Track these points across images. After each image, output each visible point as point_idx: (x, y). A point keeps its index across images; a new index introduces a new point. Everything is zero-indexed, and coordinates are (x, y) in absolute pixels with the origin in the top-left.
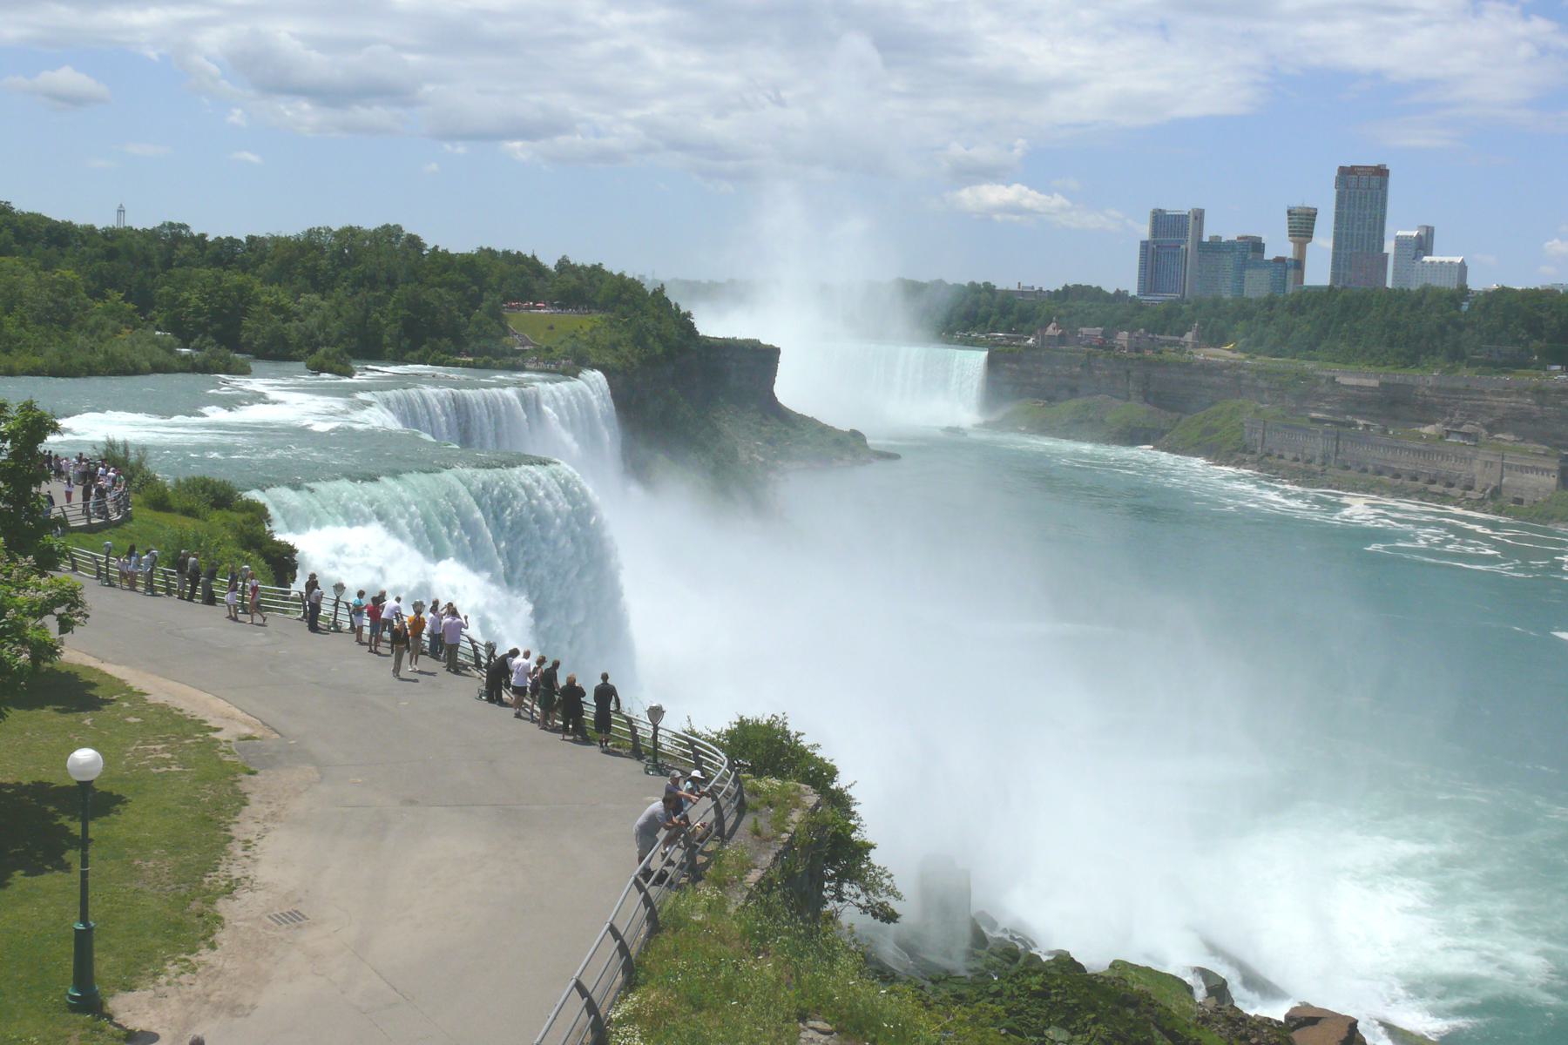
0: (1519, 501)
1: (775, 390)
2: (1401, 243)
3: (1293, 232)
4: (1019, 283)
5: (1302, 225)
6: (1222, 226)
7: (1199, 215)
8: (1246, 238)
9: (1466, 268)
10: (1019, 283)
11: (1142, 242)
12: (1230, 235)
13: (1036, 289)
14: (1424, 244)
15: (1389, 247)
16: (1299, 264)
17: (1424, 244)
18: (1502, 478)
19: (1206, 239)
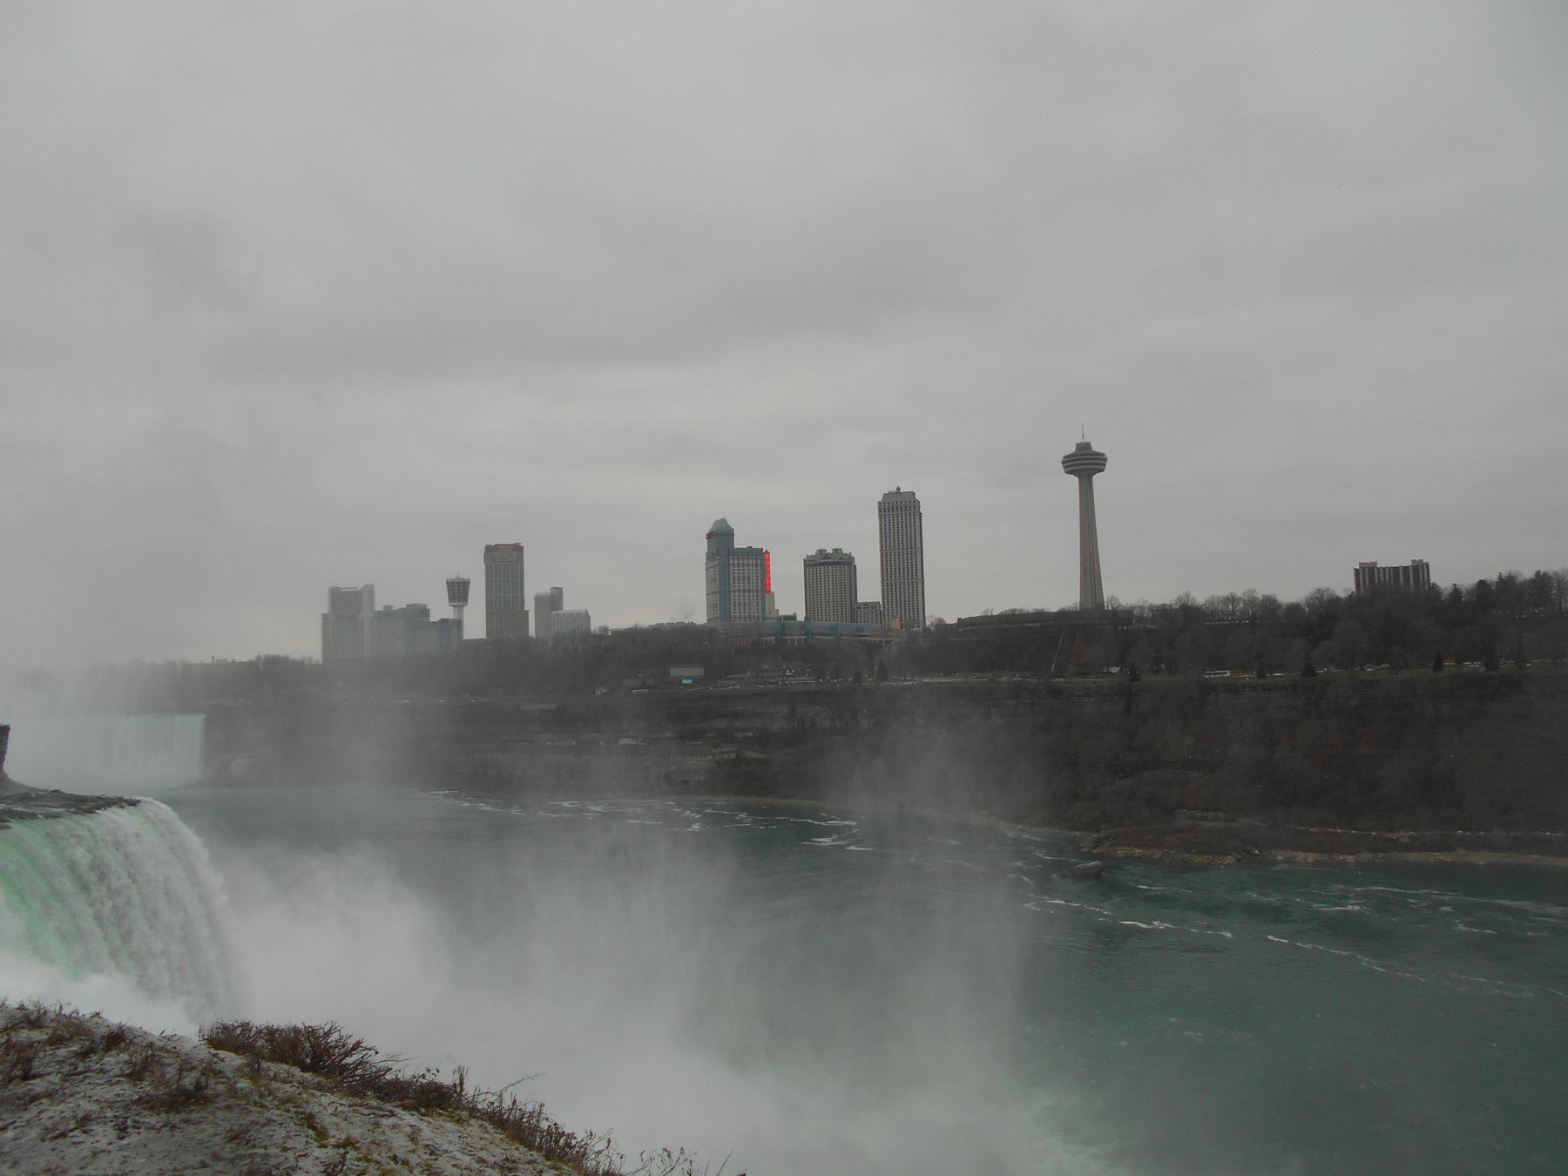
1: (4, 768)
2: (539, 600)
3: (452, 598)
4: (213, 658)
5: (458, 591)
6: (392, 596)
7: (370, 590)
8: (415, 605)
9: (589, 617)
10: (213, 658)
11: (323, 615)
12: (399, 603)
13: (230, 661)
14: (553, 599)
15: (530, 605)
16: (458, 624)
17: (553, 599)
19: (379, 607)
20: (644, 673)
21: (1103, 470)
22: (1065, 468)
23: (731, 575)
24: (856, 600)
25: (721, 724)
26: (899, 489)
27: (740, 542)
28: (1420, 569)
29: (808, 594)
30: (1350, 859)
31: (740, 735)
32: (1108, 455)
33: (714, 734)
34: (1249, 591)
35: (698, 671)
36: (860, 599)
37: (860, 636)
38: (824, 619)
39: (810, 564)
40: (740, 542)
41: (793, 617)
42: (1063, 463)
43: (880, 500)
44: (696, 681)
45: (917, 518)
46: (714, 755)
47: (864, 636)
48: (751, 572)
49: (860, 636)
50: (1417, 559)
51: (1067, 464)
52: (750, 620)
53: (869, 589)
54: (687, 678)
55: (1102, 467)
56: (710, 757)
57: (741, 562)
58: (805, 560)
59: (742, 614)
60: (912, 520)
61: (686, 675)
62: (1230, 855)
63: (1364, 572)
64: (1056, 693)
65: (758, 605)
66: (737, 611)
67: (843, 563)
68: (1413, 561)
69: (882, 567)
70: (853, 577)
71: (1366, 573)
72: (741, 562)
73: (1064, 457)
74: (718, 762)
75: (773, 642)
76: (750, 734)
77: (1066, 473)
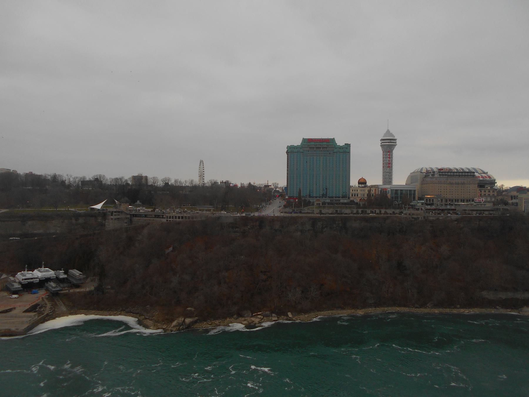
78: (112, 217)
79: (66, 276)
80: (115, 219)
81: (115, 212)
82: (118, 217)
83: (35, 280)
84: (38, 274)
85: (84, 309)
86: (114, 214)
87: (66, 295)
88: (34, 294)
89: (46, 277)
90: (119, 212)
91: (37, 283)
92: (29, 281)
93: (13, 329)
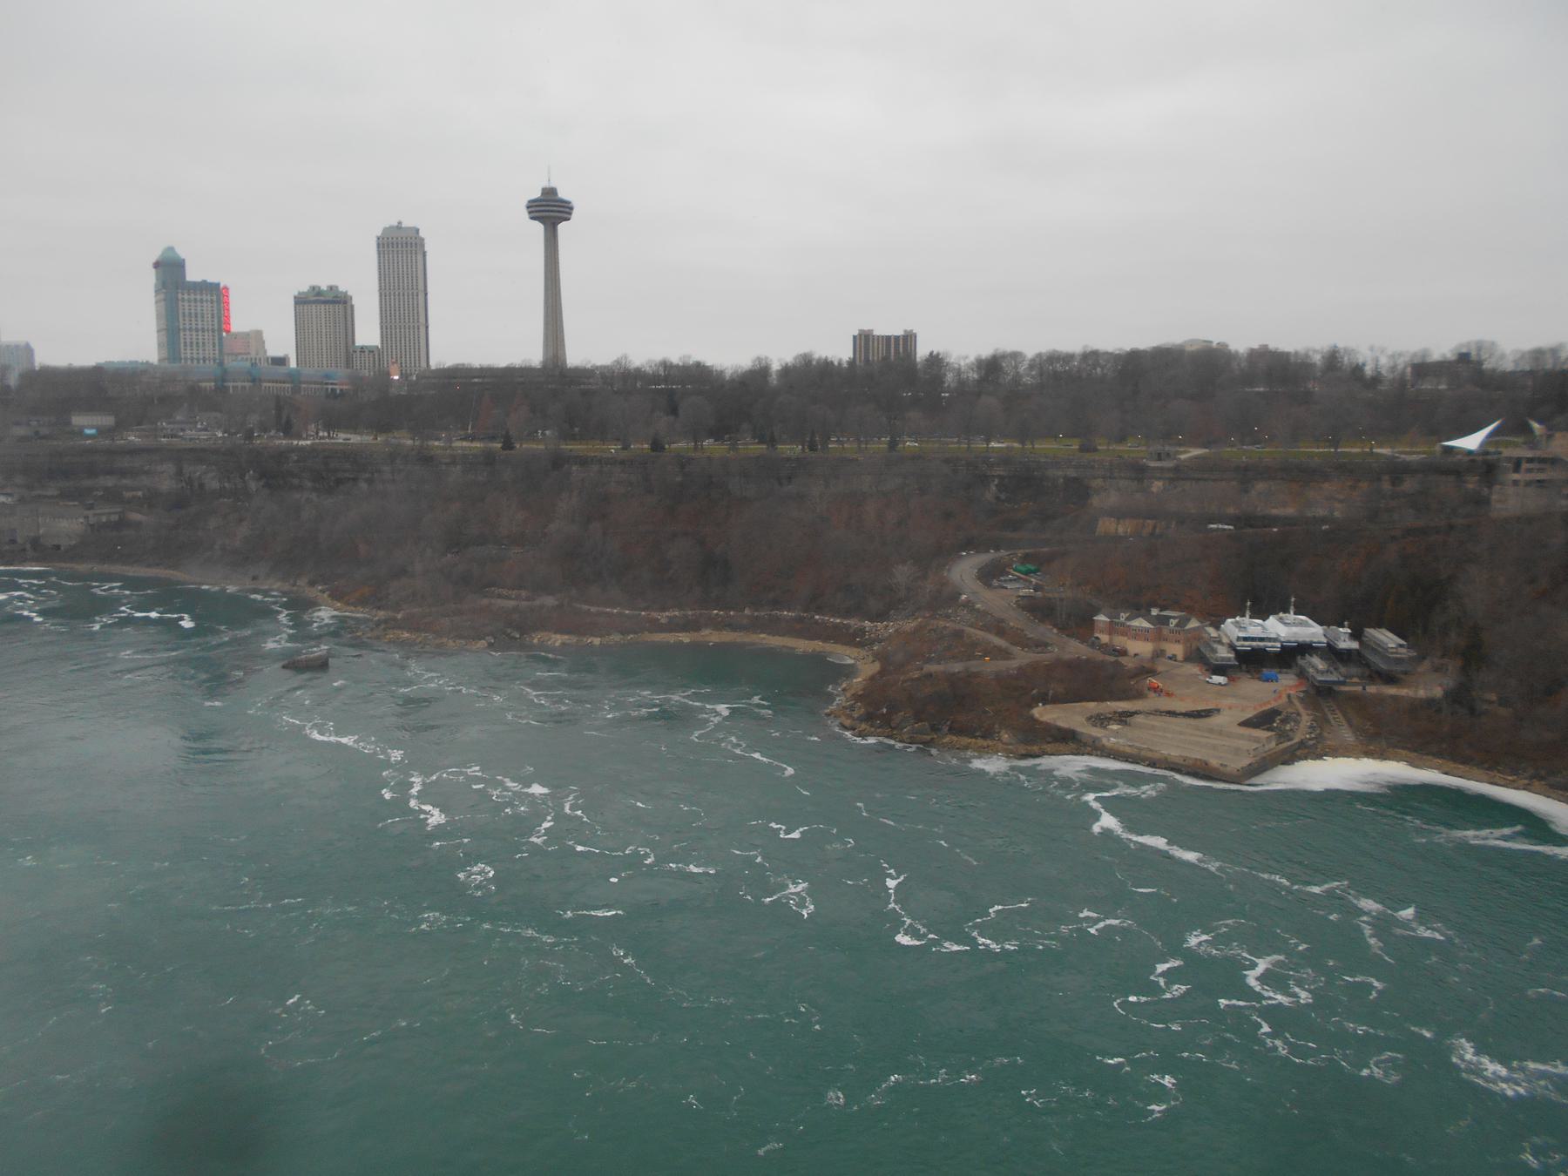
0: (58, 547)
18: (38, 530)
20: (38, 421)
21: (569, 219)
22: (530, 213)
23: (181, 312)
24: (353, 342)
25: (110, 482)
26: (400, 223)
27: (193, 275)
28: (909, 339)
29: (299, 337)
30: (597, 641)
31: (128, 495)
32: (575, 203)
33: (102, 493)
34: (684, 357)
35: (108, 420)
36: (357, 344)
37: (327, 384)
38: (316, 365)
39: (300, 301)
40: (193, 275)
41: (281, 361)
42: (528, 207)
43: (379, 234)
44: (103, 432)
45: (420, 257)
46: (86, 517)
47: (332, 384)
48: (205, 308)
49: (327, 384)
50: (909, 329)
51: (530, 210)
52: (204, 361)
53: (368, 332)
54: (91, 427)
55: (566, 216)
56: (81, 520)
57: (192, 297)
58: (295, 297)
59: (195, 356)
60: (414, 258)
61: (88, 424)
62: (484, 639)
63: (860, 339)
64: (426, 459)
65: (214, 347)
66: (189, 351)
67: (339, 302)
68: (905, 331)
69: (381, 308)
70: (349, 318)
71: (864, 340)
72: (192, 297)
73: (529, 202)
74: (91, 525)
75: (213, 388)
76: (140, 494)
77: (532, 218)
78: (1516, 476)
79: (1355, 645)
80: (1528, 484)
81: (1530, 460)
82: (1541, 476)
83: (1269, 644)
84: (1281, 629)
85: (1409, 749)
86: (1525, 466)
87: (1354, 698)
88: (1267, 681)
89: (1301, 640)
90: (1542, 460)
91: (1276, 654)
92: (1254, 644)
93: (1214, 762)
